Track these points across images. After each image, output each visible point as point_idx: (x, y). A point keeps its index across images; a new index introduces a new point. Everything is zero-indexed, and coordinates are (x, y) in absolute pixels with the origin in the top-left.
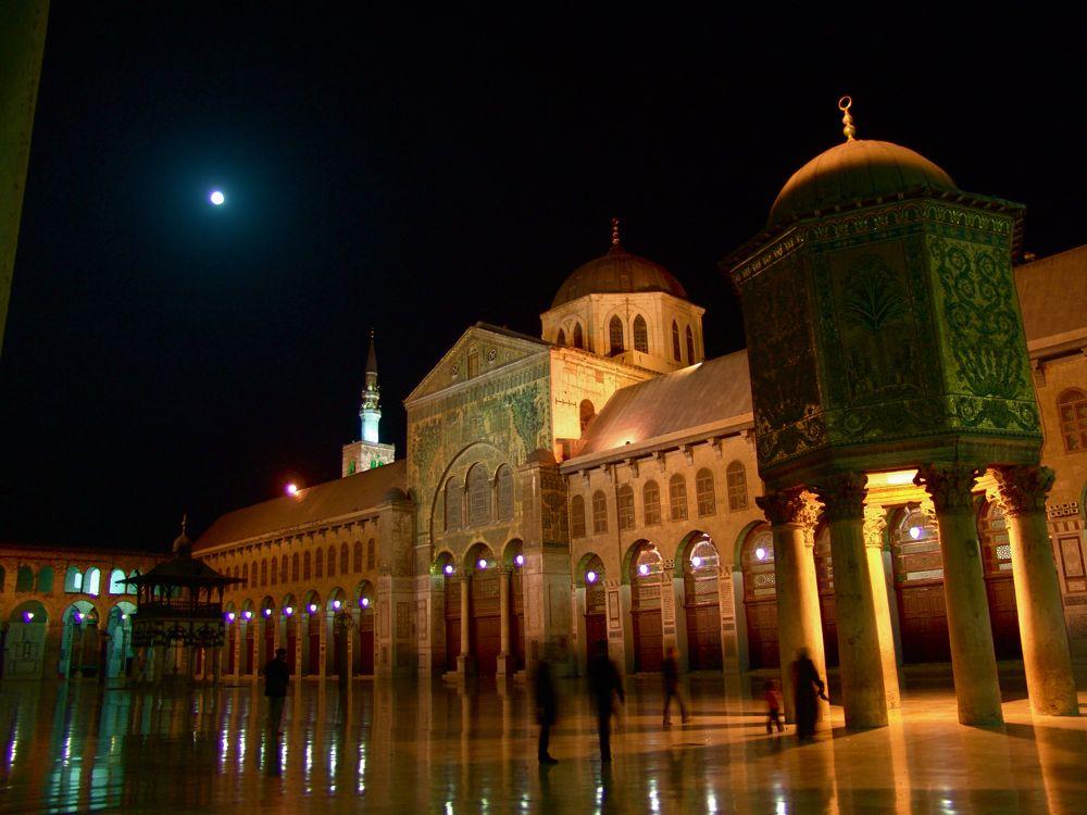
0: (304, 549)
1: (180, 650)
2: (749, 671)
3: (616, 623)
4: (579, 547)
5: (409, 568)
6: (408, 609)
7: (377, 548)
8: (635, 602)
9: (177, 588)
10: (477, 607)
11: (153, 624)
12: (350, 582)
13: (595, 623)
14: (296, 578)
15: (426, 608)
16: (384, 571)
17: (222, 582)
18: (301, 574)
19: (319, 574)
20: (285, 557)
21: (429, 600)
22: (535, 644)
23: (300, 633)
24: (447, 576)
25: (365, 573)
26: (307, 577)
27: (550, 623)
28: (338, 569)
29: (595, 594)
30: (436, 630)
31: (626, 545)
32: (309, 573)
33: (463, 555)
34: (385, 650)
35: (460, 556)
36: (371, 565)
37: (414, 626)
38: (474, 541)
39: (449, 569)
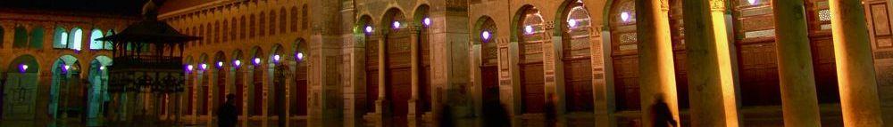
0: (250, 13)
1: (148, 96)
2: (616, 112)
3: (506, 73)
4: (475, 11)
5: (336, 28)
6: (335, 61)
7: (310, 12)
8: (522, 56)
9: (146, 45)
10: (392, 60)
11: (126, 74)
12: (288, 39)
13: (489, 73)
14: (243, 36)
15: (350, 61)
16: (315, 31)
17: (183, 40)
18: (248, 32)
19: (262, 33)
20: (234, 19)
21: (352, 55)
22: (439, 90)
23: (247, 81)
24: (367, 35)
25: (300, 32)
26: (252, 35)
27: (452, 74)
28: (278, 30)
29: (488, 50)
30: (358, 79)
31: (514, 10)
32: (254, 32)
33: (381, 18)
34: (316, 95)
35: (378, 18)
36: (305, 26)
37: (340, 76)
38: (390, 6)
39: (369, 29)
